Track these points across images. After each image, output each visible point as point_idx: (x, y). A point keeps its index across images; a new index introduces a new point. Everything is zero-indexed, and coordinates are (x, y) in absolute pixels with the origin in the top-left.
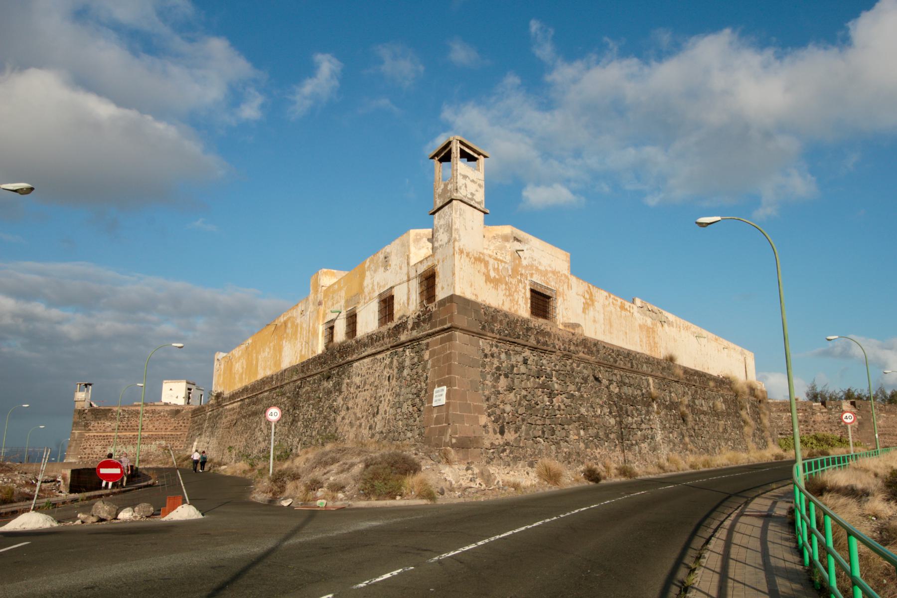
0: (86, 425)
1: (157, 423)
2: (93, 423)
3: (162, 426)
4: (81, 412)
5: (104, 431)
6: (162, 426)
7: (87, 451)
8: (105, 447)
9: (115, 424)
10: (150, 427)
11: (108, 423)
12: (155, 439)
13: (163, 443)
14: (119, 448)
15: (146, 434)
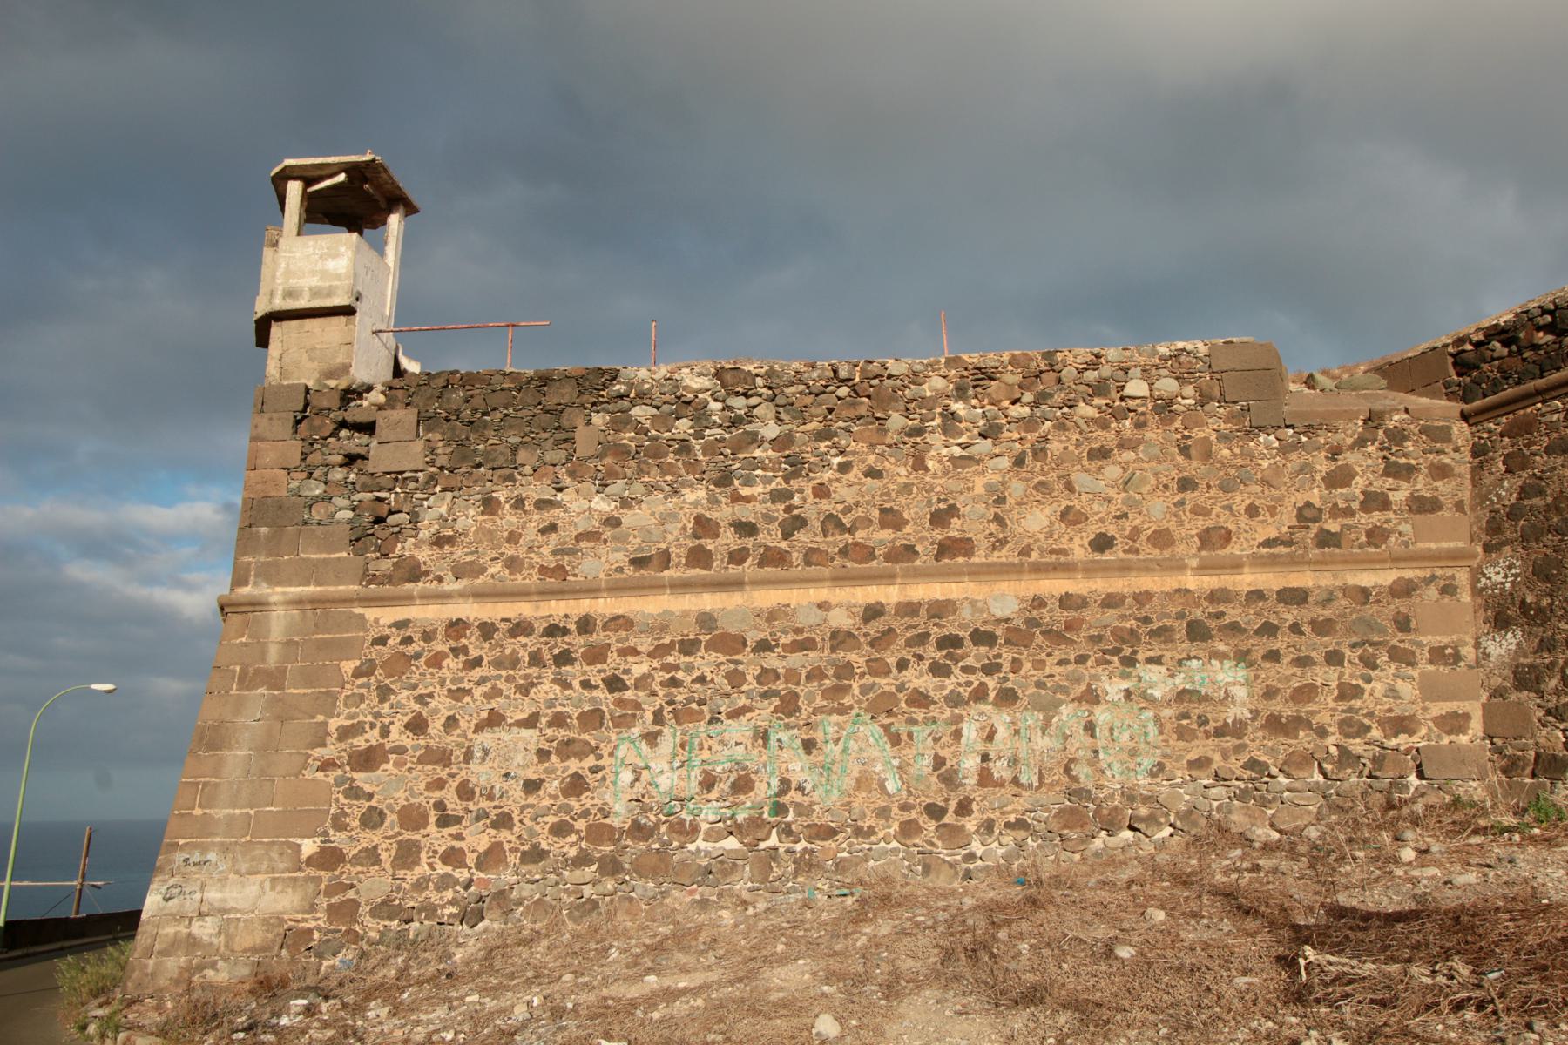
0: (375, 527)
1: (1098, 488)
2: (436, 507)
3: (1157, 510)
4: (333, 418)
5: (557, 580)
6: (1157, 510)
7: (392, 785)
8: (574, 737)
9: (663, 512)
10: (1036, 521)
11: (585, 505)
12: (1122, 650)
13: (1228, 681)
14: (730, 744)
15: (1004, 599)
